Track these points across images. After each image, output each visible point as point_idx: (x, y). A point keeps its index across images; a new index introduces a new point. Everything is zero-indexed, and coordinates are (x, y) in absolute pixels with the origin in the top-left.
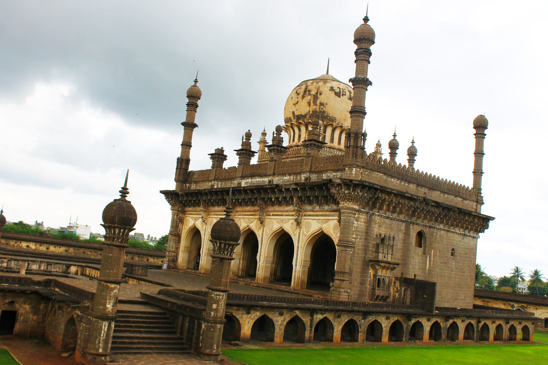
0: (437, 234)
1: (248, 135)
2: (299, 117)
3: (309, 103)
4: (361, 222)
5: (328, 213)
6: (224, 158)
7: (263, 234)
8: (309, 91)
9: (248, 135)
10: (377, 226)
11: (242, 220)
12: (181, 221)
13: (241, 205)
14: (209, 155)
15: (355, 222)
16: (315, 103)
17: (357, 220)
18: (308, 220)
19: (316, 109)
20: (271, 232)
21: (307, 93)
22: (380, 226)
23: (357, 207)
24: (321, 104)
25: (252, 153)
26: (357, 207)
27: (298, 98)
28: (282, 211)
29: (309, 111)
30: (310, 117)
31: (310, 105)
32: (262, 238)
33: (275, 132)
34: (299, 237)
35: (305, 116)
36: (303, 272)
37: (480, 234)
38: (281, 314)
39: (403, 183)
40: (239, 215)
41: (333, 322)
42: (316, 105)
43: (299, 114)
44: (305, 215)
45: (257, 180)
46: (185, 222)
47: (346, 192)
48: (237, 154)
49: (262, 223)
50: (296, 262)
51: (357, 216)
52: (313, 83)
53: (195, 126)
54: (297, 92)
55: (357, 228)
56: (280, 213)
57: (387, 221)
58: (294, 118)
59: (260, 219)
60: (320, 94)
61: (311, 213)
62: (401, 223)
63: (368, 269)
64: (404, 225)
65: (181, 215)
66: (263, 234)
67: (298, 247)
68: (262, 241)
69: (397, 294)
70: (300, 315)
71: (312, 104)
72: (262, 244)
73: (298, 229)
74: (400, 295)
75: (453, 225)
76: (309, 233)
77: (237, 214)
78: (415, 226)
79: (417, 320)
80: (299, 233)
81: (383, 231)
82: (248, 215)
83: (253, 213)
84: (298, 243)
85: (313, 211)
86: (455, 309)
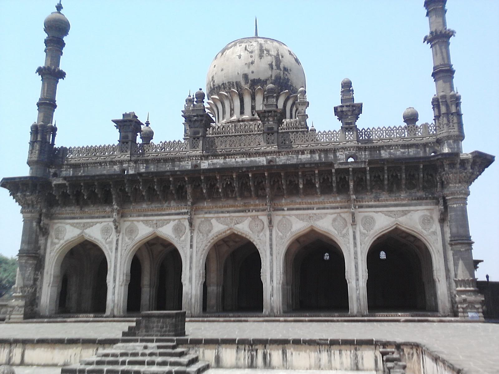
2: (255, 83)
3: (271, 65)
7: (271, 239)
8: (268, 51)
11: (214, 221)
12: (45, 232)
14: (114, 121)
16: (278, 67)
18: (366, 214)
19: (280, 74)
21: (265, 52)
24: (285, 69)
28: (311, 204)
29: (271, 76)
31: (272, 68)
32: (271, 245)
34: (355, 238)
35: (264, 82)
40: (206, 213)
42: (281, 70)
43: (256, 77)
45: (239, 160)
46: (52, 233)
49: (270, 222)
50: (357, 275)
53: (62, 75)
54: (246, 49)
58: (246, 82)
65: (44, 221)
66: (271, 239)
67: (356, 253)
68: (271, 248)
71: (274, 67)
80: (354, 232)
82: (228, 212)
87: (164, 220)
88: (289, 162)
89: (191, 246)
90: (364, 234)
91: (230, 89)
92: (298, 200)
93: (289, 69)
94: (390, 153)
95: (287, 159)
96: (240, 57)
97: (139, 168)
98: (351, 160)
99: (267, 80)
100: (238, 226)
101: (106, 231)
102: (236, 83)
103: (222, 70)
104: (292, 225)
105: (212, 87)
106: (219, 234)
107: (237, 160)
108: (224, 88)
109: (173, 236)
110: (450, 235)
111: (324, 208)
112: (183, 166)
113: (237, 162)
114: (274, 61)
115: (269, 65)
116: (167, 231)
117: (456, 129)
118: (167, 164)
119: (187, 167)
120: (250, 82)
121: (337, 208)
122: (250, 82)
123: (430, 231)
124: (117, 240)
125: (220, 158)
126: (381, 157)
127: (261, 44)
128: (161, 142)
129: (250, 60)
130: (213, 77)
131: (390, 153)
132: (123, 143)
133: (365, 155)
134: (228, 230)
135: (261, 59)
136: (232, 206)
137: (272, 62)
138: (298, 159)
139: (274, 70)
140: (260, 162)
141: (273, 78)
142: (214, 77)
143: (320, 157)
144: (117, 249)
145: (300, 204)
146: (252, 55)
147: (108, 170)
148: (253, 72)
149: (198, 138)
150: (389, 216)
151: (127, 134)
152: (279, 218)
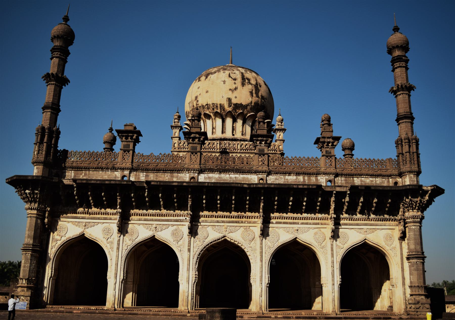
2: (237, 106)
3: (251, 93)
7: (262, 248)
8: (249, 80)
11: (209, 229)
21: (247, 81)
30: (251, 109)
31: (252, 96)
32: (261, 253)
34: (332, 250)
43: (239, 102)
50: (333, 280)
54: (230, 76)
58: (230, 106)
66: (262, 248)
67: (333, 262)
71: (254, 95)
83: (237, 220)
87: (163, 225)
88: (277, 182)
89: (189, 250)
90: (339, 247)
91: (213, 109)
94: (361, 181)
95: (276, 179)
96: (224, 82)
97: (139, 175)
98: (329, 184)
99: (247, 105)
100: (231, 234)
101: (107, 231)
102: (220, 104)
103: (207, 92)
105: (195, 106)
106: (214, 241)
107: (231, 175)
108: (208, 108)
109: (172, 240)
110: (407, 251)
111: (307, 224)
112: (181, 177)
113: (230, 178)
115: (250, 92)
116: (165, 235)
117: (416, 166)
118: (166, 174)
119: (185, 178)
120: (233, 105)
121: (318, 224)
122: (233, 105)
123: (391, 247)
124: (119, 240)
125: (216, 173)
126: (354, 183)
127: (242, 73)
128: (160, 154)
129: (234, 86)
130: (196, 98)
131: (361, 181)
132: (125, 151)
133: (341, 180)
134: (222, 238)
135: (243, 86)
138: (285, 179)
139: (253, 97)
140: (251, 179)
141: (253, 104)
142: (199, 97)
143: (304, 179)
144: (118, 249)
146: (236, 82)
147: (110, 175)
148: (236, 97)
149: (196, 153)
150: (360, 233)
151: (128, 143)
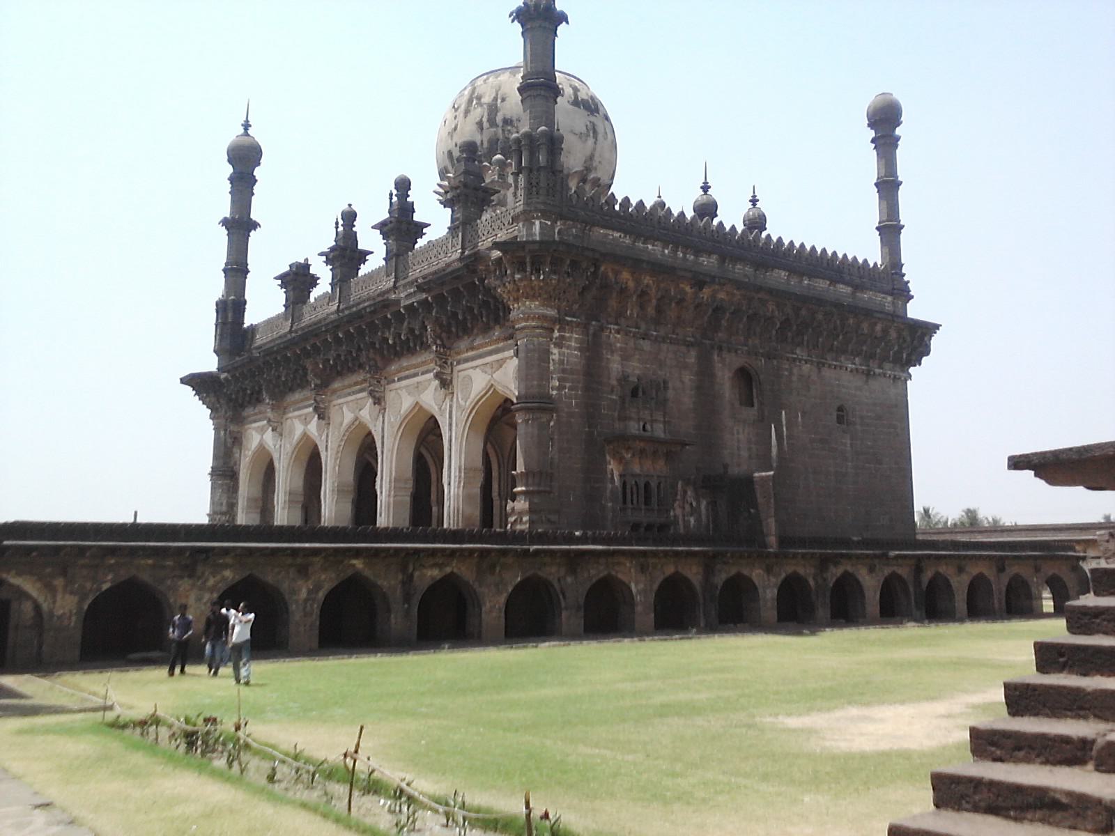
0: (791, 373)
1: (349, 217)
4: (568, 347)
5: (501, 345)
6: (313, 281)
8: (479, 98)
9: (349, 217)
10: (617, 358)
13: (340, 374)
15: (555, 351)
17: (559, 345)
20: (399, 420)
22: (625, 358)
23: (552, 312)
24: (507, 122)
25: (363, 256)
26: (552, 312)
27: (455, 117)
31: (482, 129)
32: (383, 437)
33: (395, 192)
34: (450, 417)
36: (468, 498)
37: (912, 370)
38: (303, 571)
39: (680, 255)
41: (476, 586)
44: (458, 363)
47: (517, 276)
48: (327, 262)
51: (556, 334)
52: (488, 79)
53: (255, 225)
55: (561, 362)
56: (412, 371)
57: (646, 345)
59: (371, 393)
60: (503, 100)
61: (470, 354)
62: (683, 349)
63: (606, 463)
64: (693, 353)
69: (692, 520)
70: (368, 573)
71: (486, 125)
72: (382, 452)
73: (448, 401)
74: (698, 520)
75: (831, 349)
76: (468, 403)
77: (334, 397)
78: (725, 354)
79: (733, 571)
81: (635, 368)
82: (354, 393)
84: (450, 430)
85: (472, 349)
86: (847, 543)
92: (405, 363)
93: (514, 119)
104: (401, 404)
114: (486, 114)
136: (356, 384)
137: (482, 117)
139: (485, 131)
141: (486, 145)
145: (407, 370)
146: (457, 113)
148: (456, 145)
150: (486, 372)
152: (393, 393)
